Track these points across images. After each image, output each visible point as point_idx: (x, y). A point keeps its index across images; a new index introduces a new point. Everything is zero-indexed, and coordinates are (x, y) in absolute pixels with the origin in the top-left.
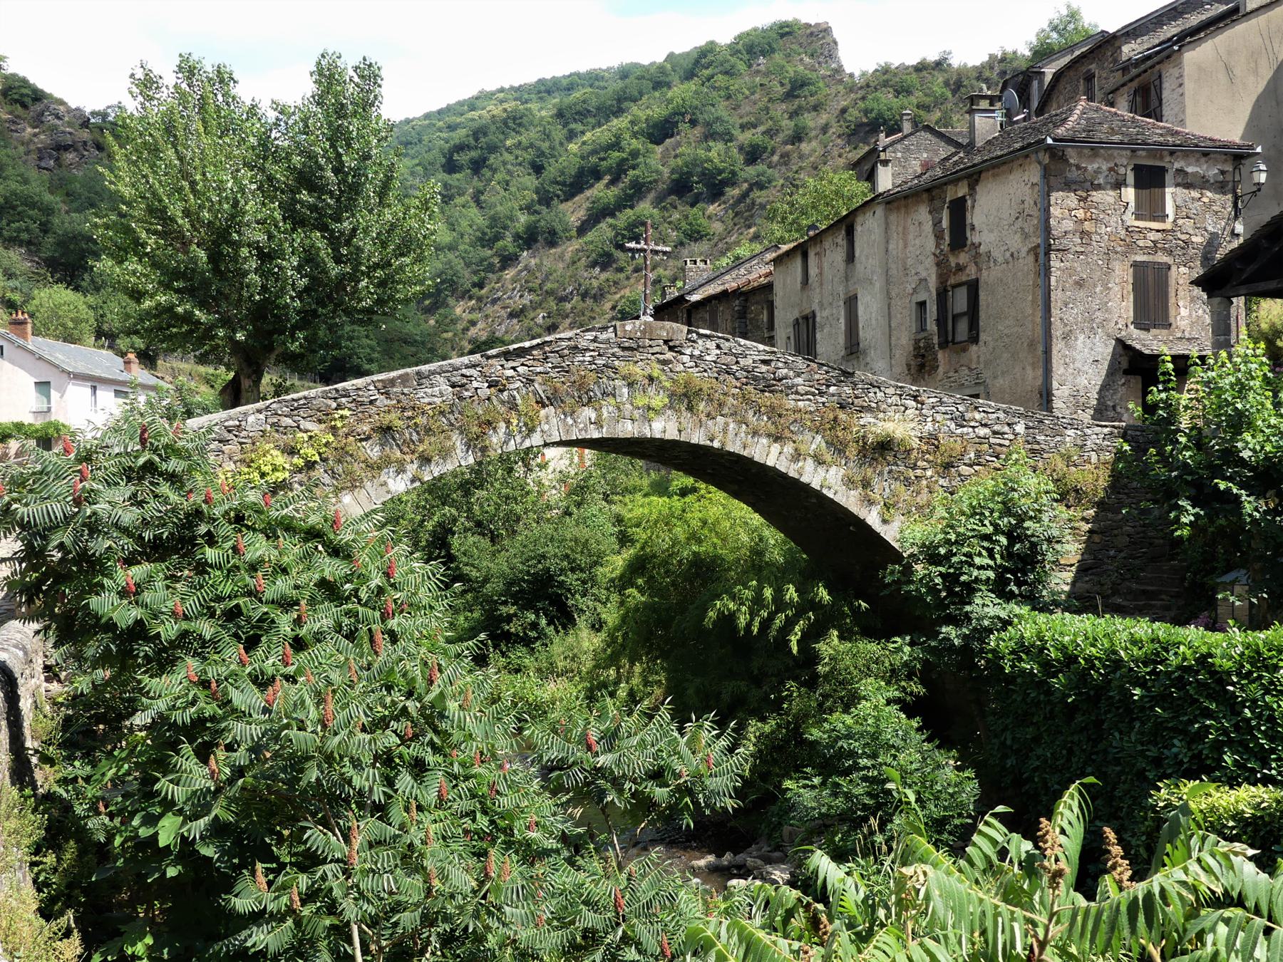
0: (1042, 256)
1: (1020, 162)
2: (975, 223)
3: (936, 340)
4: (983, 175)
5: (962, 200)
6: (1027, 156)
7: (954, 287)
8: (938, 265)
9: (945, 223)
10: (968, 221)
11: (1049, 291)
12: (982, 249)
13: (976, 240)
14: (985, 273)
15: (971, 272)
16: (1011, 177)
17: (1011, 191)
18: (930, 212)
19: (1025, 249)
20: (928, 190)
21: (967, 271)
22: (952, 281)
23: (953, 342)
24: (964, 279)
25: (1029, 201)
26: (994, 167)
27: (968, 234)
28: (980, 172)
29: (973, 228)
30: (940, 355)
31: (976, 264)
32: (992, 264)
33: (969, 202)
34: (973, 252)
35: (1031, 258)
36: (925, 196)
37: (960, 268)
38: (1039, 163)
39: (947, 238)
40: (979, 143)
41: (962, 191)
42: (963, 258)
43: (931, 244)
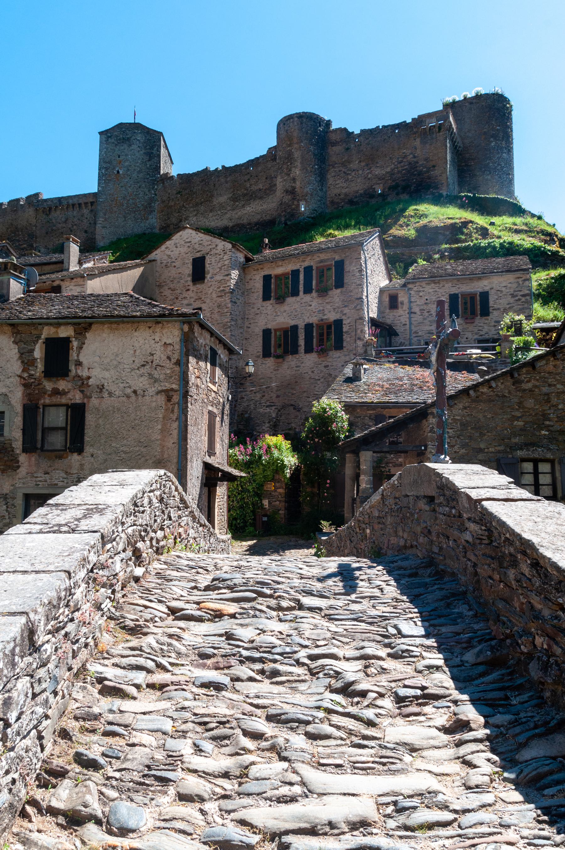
0: (176, 398)
1: (149, 324)
2: (82, 359)
3: (18, 445)
4: (94, 327)
5: (67, 341)
6: (158, 323)
7: (45, 406)
8: (25, 385)
9: (38, 352)
10: (73, 355)
11: (186, 426)
12: (91, 382)
13: (84, 373)
14: (94, 402)
15: (78, 398)
16: (136, 334)
17: (136, 344)
18: (15, 342)
19: (152, 391)
20: (12, 325)
21: (70, 396)
22: (47, 401)
23: (42, 449)
24: (64, 401)
25: (160, 356)
26: (117, 323)
27: (72, 367)
28: (90, 324)
29: (79, 364)
30: (23, 458)
31: (82, 392)
32: (106, 395)
33: (75, 344)
34: (80, 383)
35: (161, 399)
36: (7, 329)
37: (56, 392)
38: (182, 330)
39: (40, 366)
40: (12, 299)
41: (65, 332)
42: (62, 385)
43: (16, 367)
